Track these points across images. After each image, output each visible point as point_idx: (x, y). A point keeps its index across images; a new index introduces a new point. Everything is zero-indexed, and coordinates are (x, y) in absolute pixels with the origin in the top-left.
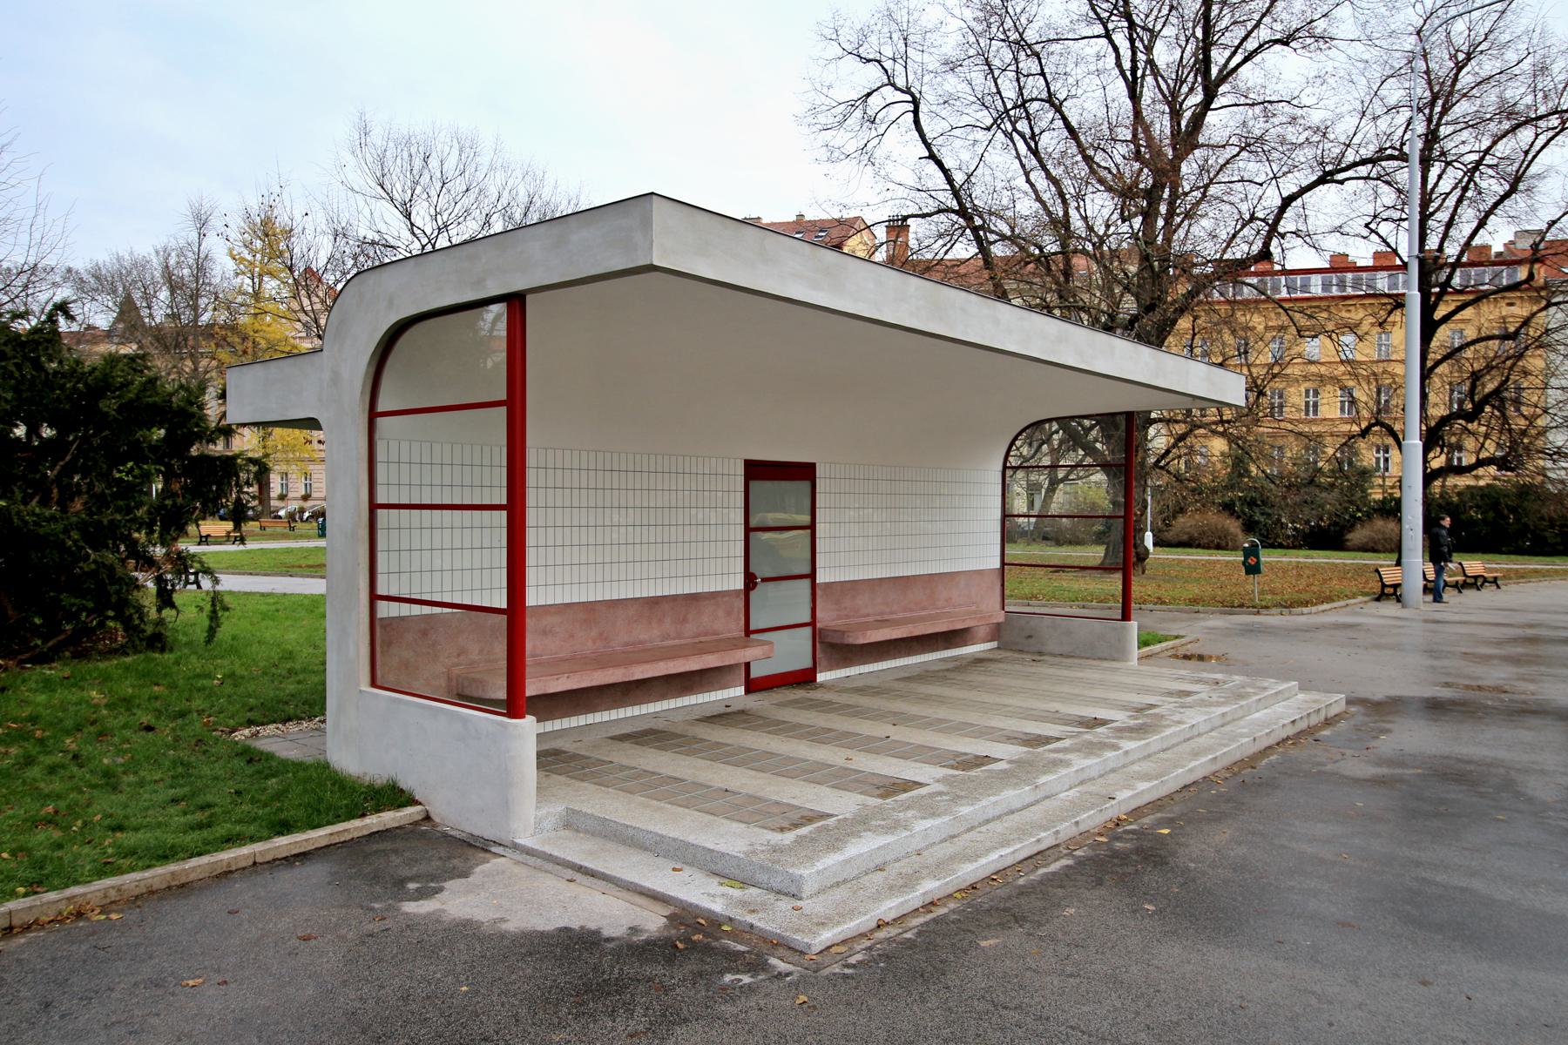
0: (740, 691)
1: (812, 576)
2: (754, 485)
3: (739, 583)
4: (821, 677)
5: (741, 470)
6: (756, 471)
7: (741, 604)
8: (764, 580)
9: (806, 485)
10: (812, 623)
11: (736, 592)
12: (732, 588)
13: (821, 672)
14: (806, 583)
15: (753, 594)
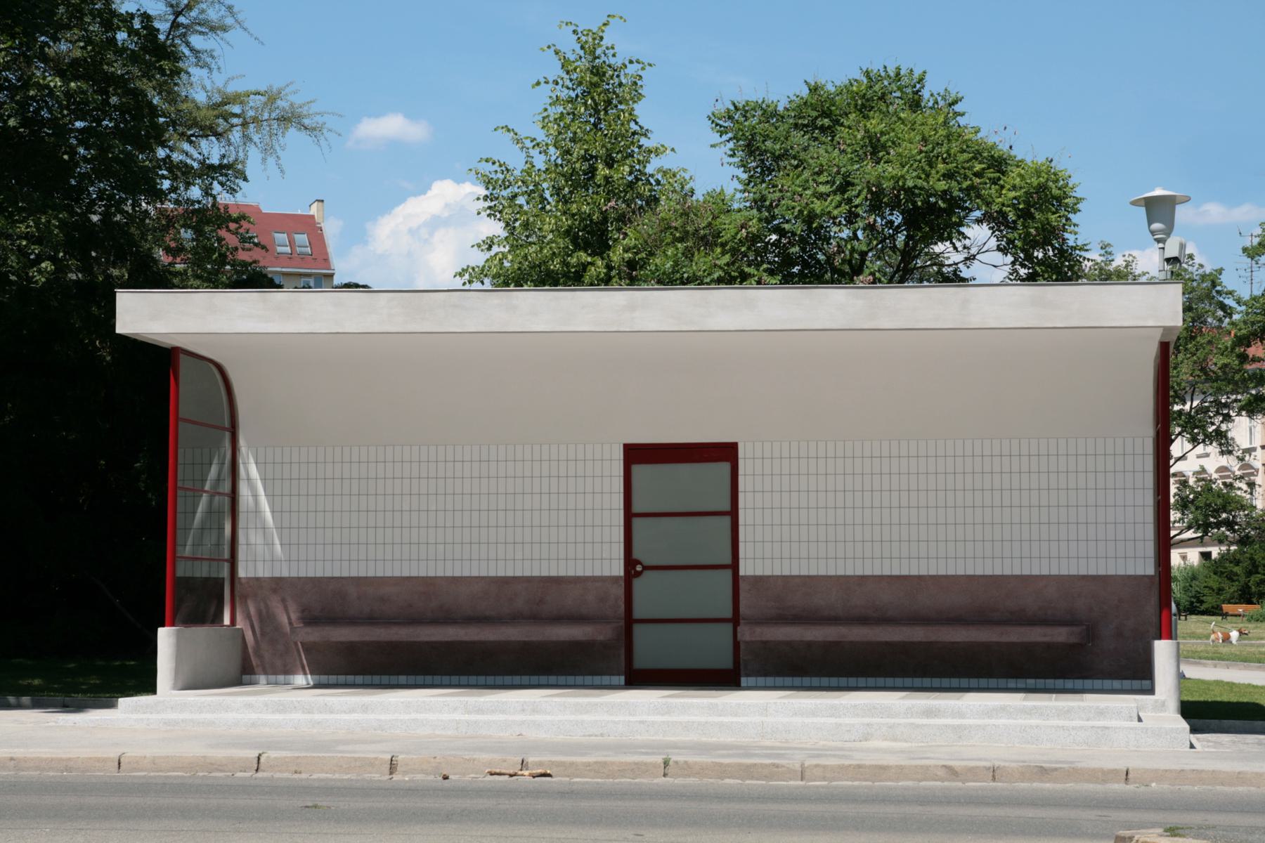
0: (622, 678)
1: (734, 565)
2: (637, 470)
3: (618, 569)
4: (744, 681)
5: (619, 454)
6: (636, 454)
7: (620, 591)
8: (646, 568)
9: (725, 467)
10: (735, 620)
11: (614, 579)
12: (606, 573)
13: (748, 675)
14: (728, 574)
15: (637, 584)
